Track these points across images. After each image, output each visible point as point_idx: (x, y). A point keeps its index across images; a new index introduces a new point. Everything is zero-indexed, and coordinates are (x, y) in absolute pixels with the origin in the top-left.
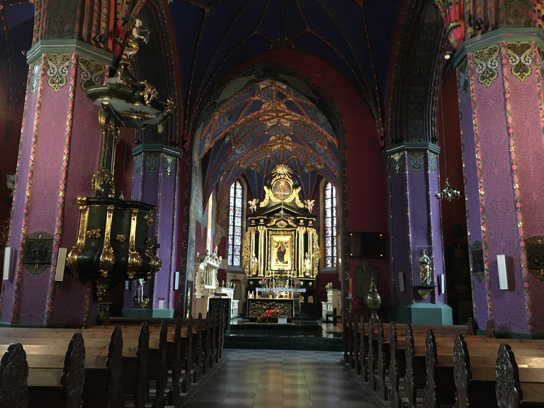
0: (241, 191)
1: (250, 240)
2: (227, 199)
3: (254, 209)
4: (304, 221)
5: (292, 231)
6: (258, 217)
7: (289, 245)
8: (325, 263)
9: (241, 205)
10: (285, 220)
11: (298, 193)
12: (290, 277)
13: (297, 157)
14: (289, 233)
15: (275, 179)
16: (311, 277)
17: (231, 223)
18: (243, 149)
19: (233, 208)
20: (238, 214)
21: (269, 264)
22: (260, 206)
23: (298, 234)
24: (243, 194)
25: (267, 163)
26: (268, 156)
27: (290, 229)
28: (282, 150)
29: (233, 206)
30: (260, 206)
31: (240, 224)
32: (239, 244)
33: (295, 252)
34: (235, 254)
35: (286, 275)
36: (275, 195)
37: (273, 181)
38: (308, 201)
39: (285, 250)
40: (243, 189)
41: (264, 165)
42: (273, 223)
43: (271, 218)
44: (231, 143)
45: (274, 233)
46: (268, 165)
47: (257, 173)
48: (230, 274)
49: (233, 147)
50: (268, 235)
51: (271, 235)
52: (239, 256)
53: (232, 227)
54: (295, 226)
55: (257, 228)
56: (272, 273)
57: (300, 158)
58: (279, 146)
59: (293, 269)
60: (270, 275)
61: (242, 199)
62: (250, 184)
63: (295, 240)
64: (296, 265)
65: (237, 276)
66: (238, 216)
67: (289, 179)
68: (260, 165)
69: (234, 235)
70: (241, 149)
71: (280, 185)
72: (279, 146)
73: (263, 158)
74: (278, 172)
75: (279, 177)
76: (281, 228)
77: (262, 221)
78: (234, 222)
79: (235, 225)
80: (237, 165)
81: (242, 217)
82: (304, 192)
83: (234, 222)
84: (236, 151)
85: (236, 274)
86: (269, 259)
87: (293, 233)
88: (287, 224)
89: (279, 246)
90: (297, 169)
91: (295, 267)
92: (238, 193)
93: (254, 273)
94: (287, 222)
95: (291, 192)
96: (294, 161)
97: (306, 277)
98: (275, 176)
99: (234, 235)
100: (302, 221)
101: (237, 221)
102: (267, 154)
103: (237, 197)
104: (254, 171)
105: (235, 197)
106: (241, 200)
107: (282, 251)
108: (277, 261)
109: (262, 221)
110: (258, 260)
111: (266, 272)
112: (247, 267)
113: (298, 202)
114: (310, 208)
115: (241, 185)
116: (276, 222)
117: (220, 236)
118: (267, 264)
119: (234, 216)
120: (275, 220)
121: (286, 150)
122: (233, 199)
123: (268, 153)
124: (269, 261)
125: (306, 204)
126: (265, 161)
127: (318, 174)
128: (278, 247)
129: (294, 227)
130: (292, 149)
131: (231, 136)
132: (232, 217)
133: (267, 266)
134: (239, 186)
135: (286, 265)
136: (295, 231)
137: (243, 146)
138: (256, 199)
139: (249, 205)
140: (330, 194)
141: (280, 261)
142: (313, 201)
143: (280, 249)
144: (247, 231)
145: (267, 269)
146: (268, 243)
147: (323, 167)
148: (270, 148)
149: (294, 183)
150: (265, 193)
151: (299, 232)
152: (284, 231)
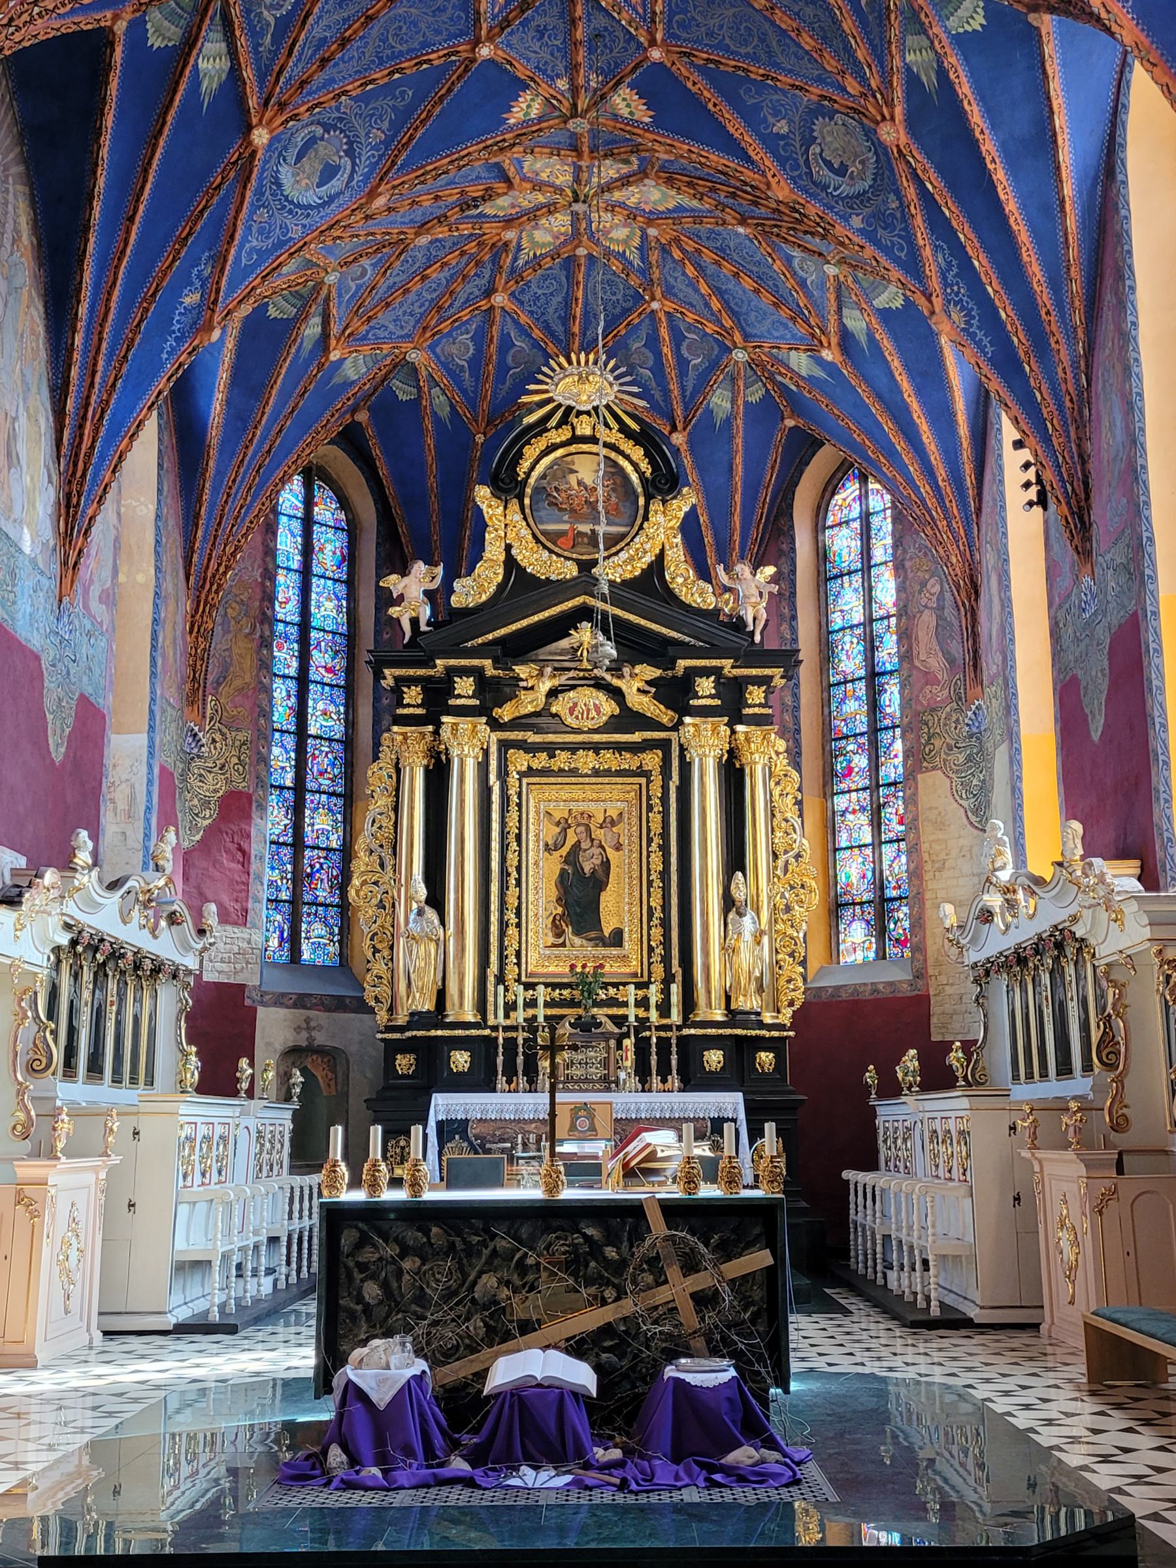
0: (343, 536)
1: (396, 809)
2: (257, 574)
3: (415, 622)
7: (627, 831)
9: (343, 618)
10: (600, 685)
11: (675, 523)
12: (643, 1023)
13: (669, 306)
14: (629, 761)
15: (541, 444)
16: (768, 1018)
17: (282, 713)
18: (329, 172)
19: (293, 631)
20: (329, 670)
21: (511, 952)
22: (455, 601)
24: (351, 558)
26: (499, 299)
27: (637, 737)
28: (581, 252)
29: (296, 619)
30: (455, 601)
31: (338, 730)
33: (665, 875)
34: (307, 898)
35: (620, 1011)
36: (546, 541)
37: (530, 452)
38: (743, 569)
40: (352, 531)
41: (476, 363)
42: (528, 703)
43: (522, 671)
44: (242, 100)
45: (541, 761)
46: (503, 368)
47: (434, 413)
48: (280, 1013)
49: (261, 137)
50: (503, 774)
51: (522, 774)
52: (333, 911)
53: (290, 741)
54: (666, 716)
55: (436, 733)
56: (531, 1004)
57: (691, 317)
58: (560, 222)
59: (659, 971)
60: (520, 1016)
62: (390, 490)
63: (665, 800)
64: (675, 952)
65: (319, 1028)
66: (328, 678)
67: (627, 446)
69: (299, 787)
70: (312, 165)
71: (573, 479)
72: (560, 222)
73: (465, 315)
74: (560, 399)
75: (565, 434)
76: (578, 731)
77: (465, 686)
78: (301, 714)
79: (312, 730)
80: (308, 345)
81: (350, 691)
82: (708, 539)
83: (301, 714)
84: (286, 174)
85: (313, 1013)
86: (511, 916)
87: (652, 760)
88: (609, 707)
89: (571, 839)
90: (666, 392)
91: (666, 960)
92: (329, 548)
93: (427, 1005)
94: (616, 694)
95: (637, 520)
96: (653, 342)
97: (734, 1016)
98: (541, 427)
99: (299, 787)
100: (705, 686)
101: (321, 706)
102: (489, 292)
103: (316, 570)
104: (416, 403)
105: (306, 572)
106: (342, 589)
108: (559, 933)
109: (465, 686)
110: (443, 922)
111: (497, 996)
112: (379, 967)
114: (755, 612)
115: (344, 503)
116: (553, 693)
117: (214, 786)
118: (502, 948)
119: (303, 680)
120: (545, 686)
121: (608, 253)
122: (294, 578)
123: (501, 282)
124: (512, 931)
125: (728, 589)
126: (481, 338)
127: (790, 423)
128: (564, 851)
129: (660, 727)
130: (643, 249)
131: (242, 41)
132: (292, 685)
133: (502, 958)
134: (326, 511)
135: (615, 951)
136: (665, 745)
137: (330, 149)
138: (430, 562)
139: (386, 599)
140: (856, 544)
141: (577, 933)
142: (770, 570)
143: (572, 857)
144: (376, 758)
145: (500, 979)
146: (503, 824)
147: (827, 355)
148: (510, 235)
149: (652, 463)
150: (481, 526)
152: (596, 748)
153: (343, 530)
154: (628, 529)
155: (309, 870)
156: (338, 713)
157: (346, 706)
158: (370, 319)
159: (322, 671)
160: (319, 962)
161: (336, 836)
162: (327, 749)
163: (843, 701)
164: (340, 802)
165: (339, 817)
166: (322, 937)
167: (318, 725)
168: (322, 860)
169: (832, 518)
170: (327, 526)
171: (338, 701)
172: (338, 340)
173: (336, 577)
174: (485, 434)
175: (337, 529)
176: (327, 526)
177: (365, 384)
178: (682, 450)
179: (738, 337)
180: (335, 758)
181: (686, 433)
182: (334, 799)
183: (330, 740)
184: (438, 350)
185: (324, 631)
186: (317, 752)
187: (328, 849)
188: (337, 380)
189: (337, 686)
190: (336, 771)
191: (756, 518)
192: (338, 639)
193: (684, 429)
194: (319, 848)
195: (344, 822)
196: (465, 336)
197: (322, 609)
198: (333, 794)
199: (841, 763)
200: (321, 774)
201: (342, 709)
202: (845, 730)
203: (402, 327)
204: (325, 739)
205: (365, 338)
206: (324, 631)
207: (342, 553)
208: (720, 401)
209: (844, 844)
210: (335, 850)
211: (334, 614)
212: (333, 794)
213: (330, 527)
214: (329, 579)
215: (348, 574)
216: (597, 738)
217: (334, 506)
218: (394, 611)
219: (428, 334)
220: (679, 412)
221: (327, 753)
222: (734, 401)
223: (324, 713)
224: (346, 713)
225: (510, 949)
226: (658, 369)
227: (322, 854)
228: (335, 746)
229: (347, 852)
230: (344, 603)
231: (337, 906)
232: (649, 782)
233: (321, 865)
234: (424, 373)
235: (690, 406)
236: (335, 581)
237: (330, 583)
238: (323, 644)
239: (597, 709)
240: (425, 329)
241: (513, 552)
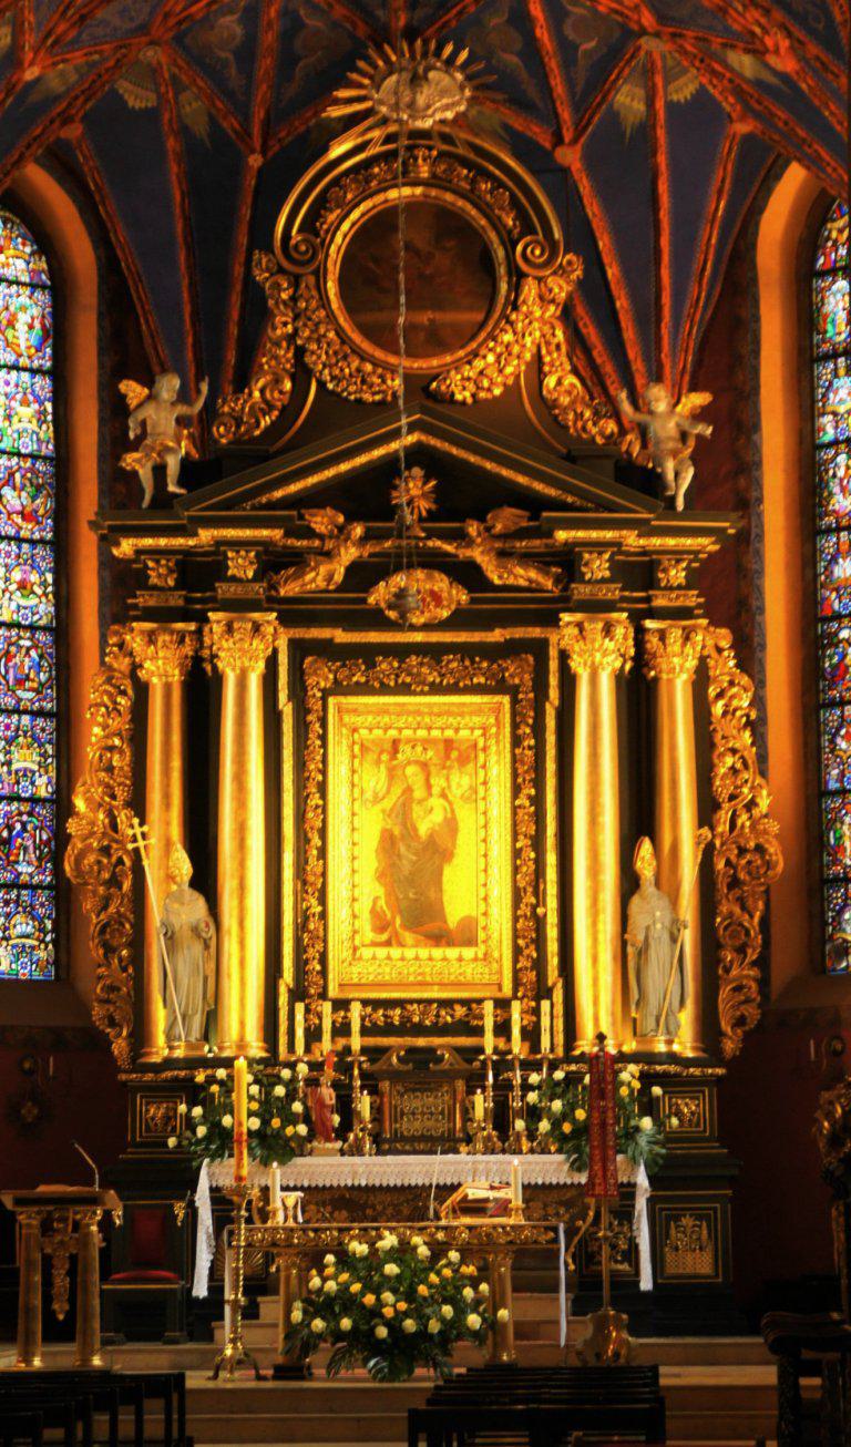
0: (42, 297)
3: (160, 471)
4: (614, 566)
5: (511, 649)
6: (206, 536)
8: (824, 939)
9: (47, 432)
20: (26, 516)
23: (568, 682)
25: (269, 39)
31: (44, 610)
32: (43, 788)
39: (451, 825)
41: (247, 54)
46: (287, 60)
47: (184, 131)
52: (43, 896)
61: (60, 374)
62: (121, 235)
68: (202, 62)
82: (622, 303)
87: (517, 672)
92: (23, 319)
94: (467, 575)
104: (151, 115)
106: (43, 385)
107: (423, 829)
113: (561, 382)
115: (44, 241)
127: (742, 128)
136: (539, 648)
151: (578, 665)
152: (434, 652)
153: (43, 287)
154: (480, 317)
155: (5, 834)
156: (44, 584)
157: (56, 572)
158: (83, 18)
159: (18, 519)
160: (24, 974)
161: (45, 779)
162: (28, 643)
163: (834, 560)
164: (50, 725)
165: (50, 749)
166: (28, 937)
167: (13, 606)
168: (25, 818)
169: (821, 261)
170: (18, 283)
171: (43, 565)
172: (36, 51)
173: (36, 364)
174: (264, 152)
175: (33, 286)
176: (18, 283)
177: (76, 98)
178: (574, 168)
179: (648, 19)
180: (41, 657)
181: (578, 147)
182: (40, 722)
183: (32, 628)
184: (187, 41)
185: (19, 454)
186: (13, 649)
187: (33, 800)
188: (33, 98)
189: (42, 541)
190: (43, 677)
191: (696, 266)
192: (40, 466)
193: (575, 141)
194: (20, 799)
195: (58, 755)
196: (229, 18)
197: (15, 419)
198: (40, 713)
199: (831, 657)
200: (20, 682)
201: (50, 577)
202: (836, 606)
203: (131, 19)
204: (25, 628)
205: (76, 40)
206: (19, 454)
207: (43, 327)
208: (628, 100)
209: (833, 785)
210: (44, 801)
211: (34, 426)
212: (40, 713)
213: (24, 284)
214: (25, 369)
215: (56, 357)
216: (435, 637)
217: (28, 250)
218: (130, 460)
219: (172, 21)
220: (566, 114)
221: (28, 649)
222: (650, 102)
223: (22, 585)
224: (56, 582)
225: (311, 950)
226: (531, 51)
227: (25, 807)
228: (39, 636)
229: (61, 805)
230: (49, 406)
231: (48, 887)
232: (515, 702)
233: (24, 825)
234: (167, 76)
235: (582, 107)
236: (33, 372)
237: (25, 376)
238: (18, 475)
239: (437, 598)
240: (167, 16)
241: (309, 359)
